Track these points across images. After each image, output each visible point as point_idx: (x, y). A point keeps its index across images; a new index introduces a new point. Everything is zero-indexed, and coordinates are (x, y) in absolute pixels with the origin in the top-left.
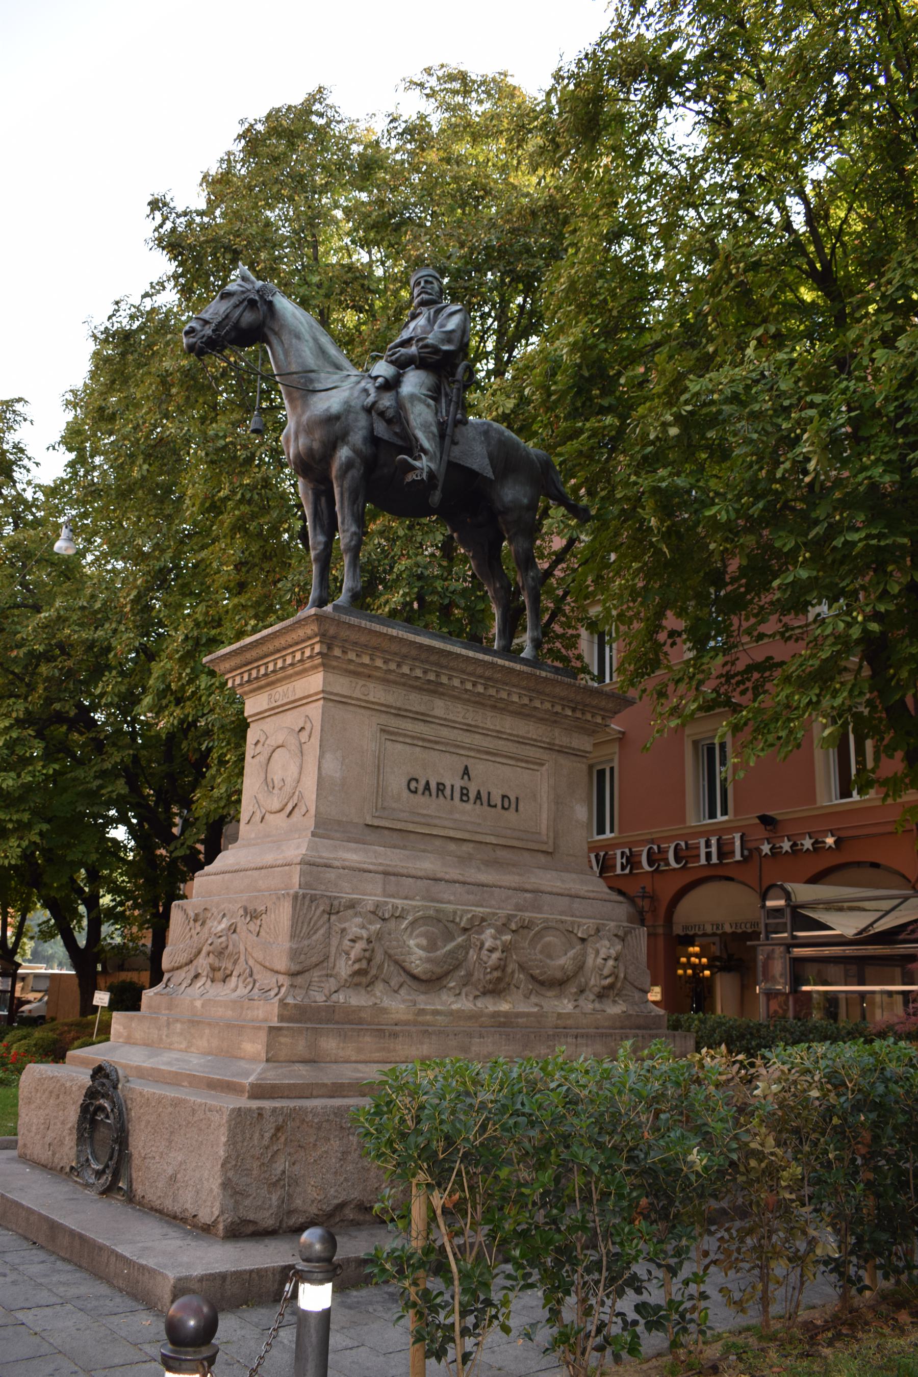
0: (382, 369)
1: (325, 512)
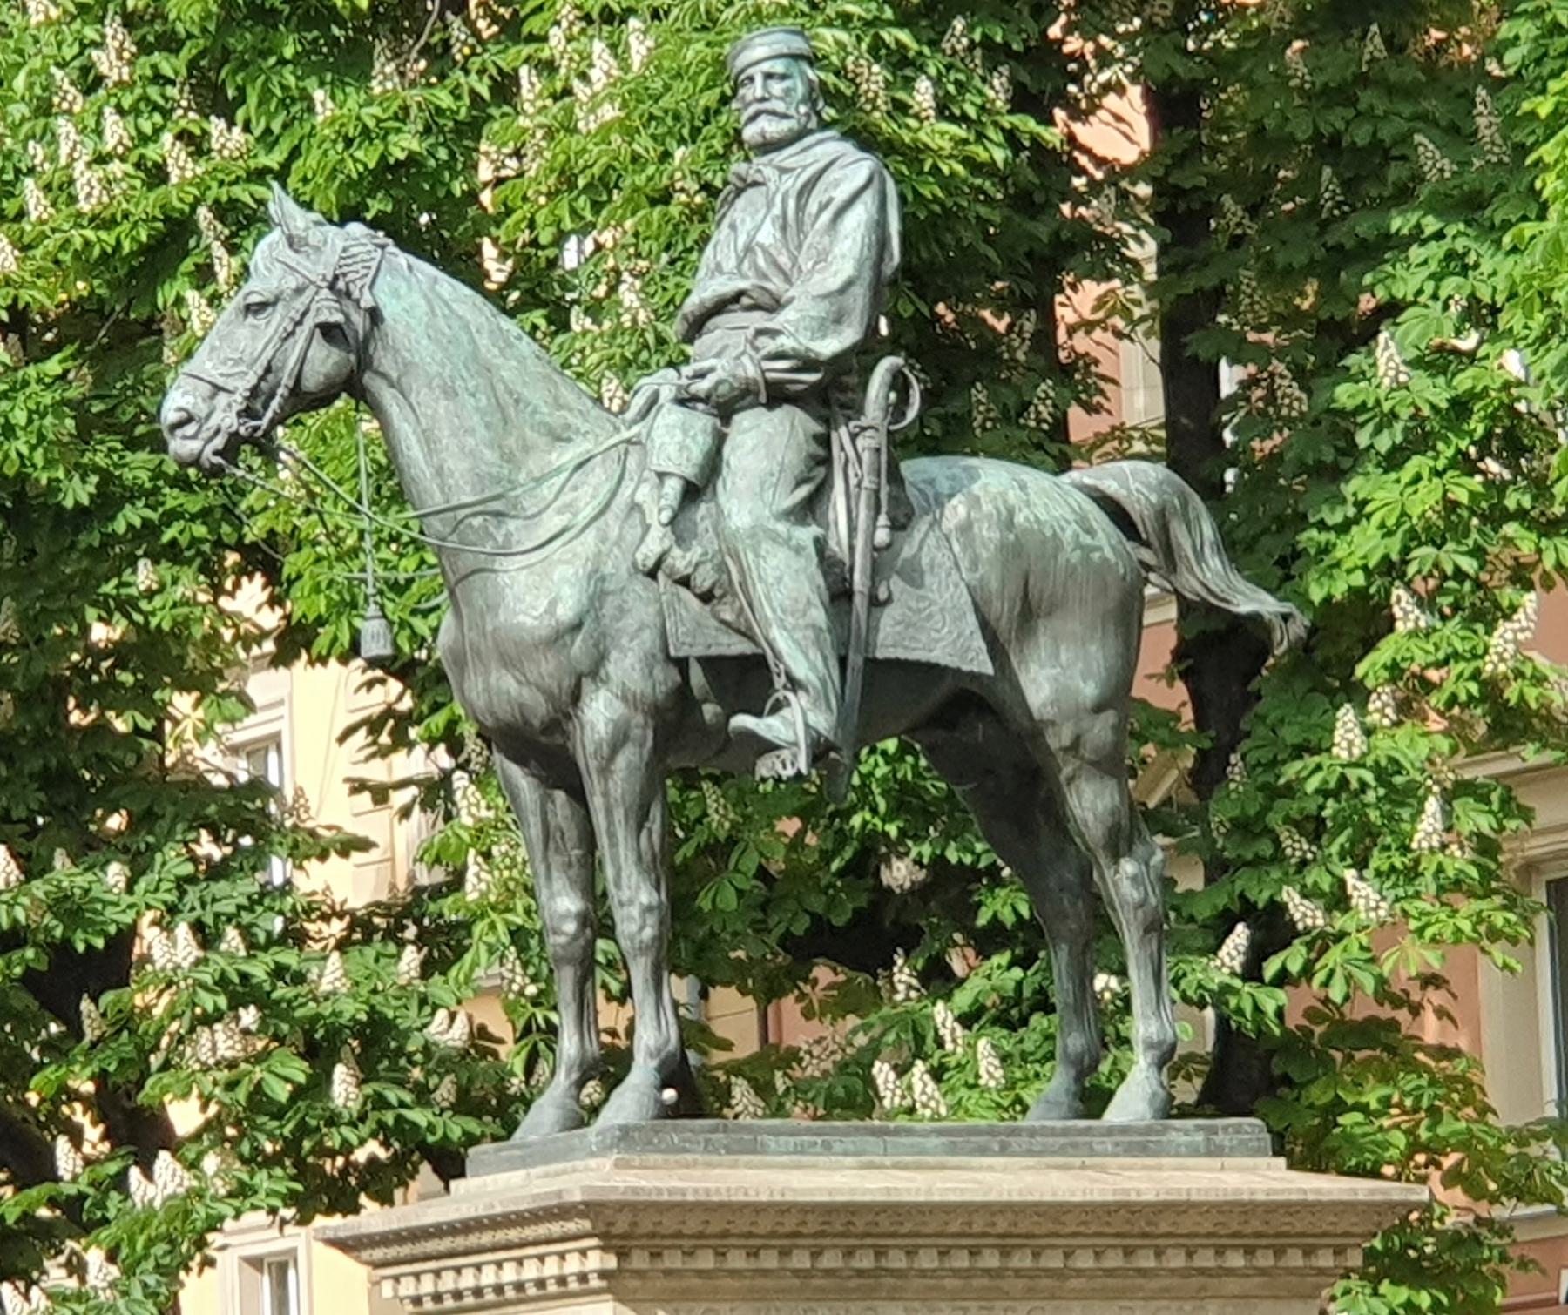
0: (676, 440)
1: (572, 834)
